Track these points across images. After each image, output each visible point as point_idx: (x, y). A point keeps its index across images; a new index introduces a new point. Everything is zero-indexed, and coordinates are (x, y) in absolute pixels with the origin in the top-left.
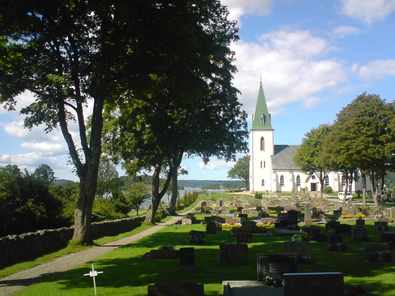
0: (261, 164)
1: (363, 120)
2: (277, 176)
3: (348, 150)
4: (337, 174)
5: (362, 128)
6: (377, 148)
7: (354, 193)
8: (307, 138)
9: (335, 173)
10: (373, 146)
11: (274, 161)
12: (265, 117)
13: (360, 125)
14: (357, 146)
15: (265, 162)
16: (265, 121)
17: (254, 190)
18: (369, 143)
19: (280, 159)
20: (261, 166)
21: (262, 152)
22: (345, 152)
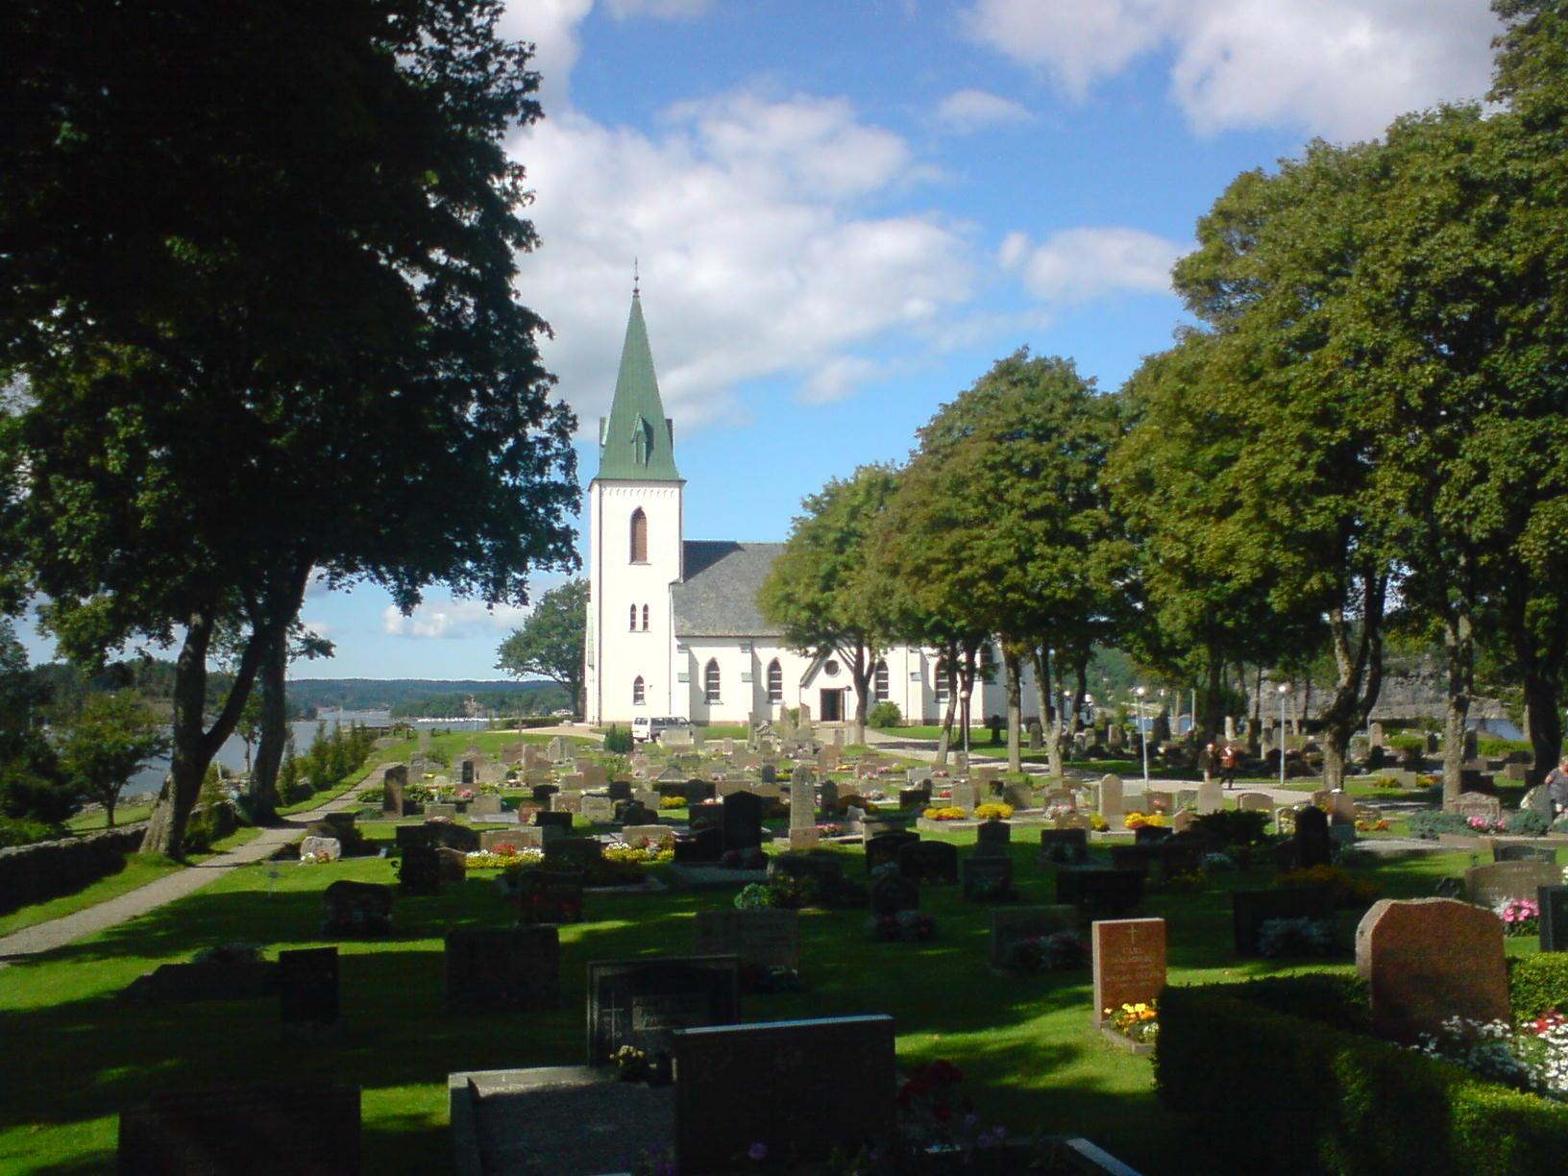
0: (633, 617)
1: (1013, 451)
2: (693, 662)
3: (959, 564)
4: (918, 655)
5: (1007, 482)
6: (1061, 561)
7: (980, 726)
8: (810, 515)
9: (912, 652)
10: (1048, 551)
11: (683, 602)
12: (648, 429)
13: (1001, 471)
14: (989, 551)
15: (646, 608)
16: (650, 446)
17: (604, 719)
18: (1031, 540)
20: (633, 625)
21: (637, 568)
22: (946, 572)
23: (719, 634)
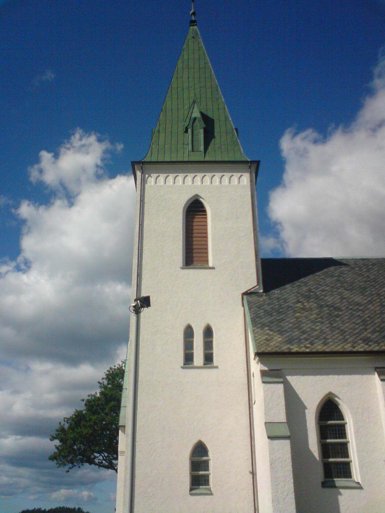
16: (209, 135)
19: (299, 305)
20: (188, 359)
21: (192, 273)
23: (339, 348)
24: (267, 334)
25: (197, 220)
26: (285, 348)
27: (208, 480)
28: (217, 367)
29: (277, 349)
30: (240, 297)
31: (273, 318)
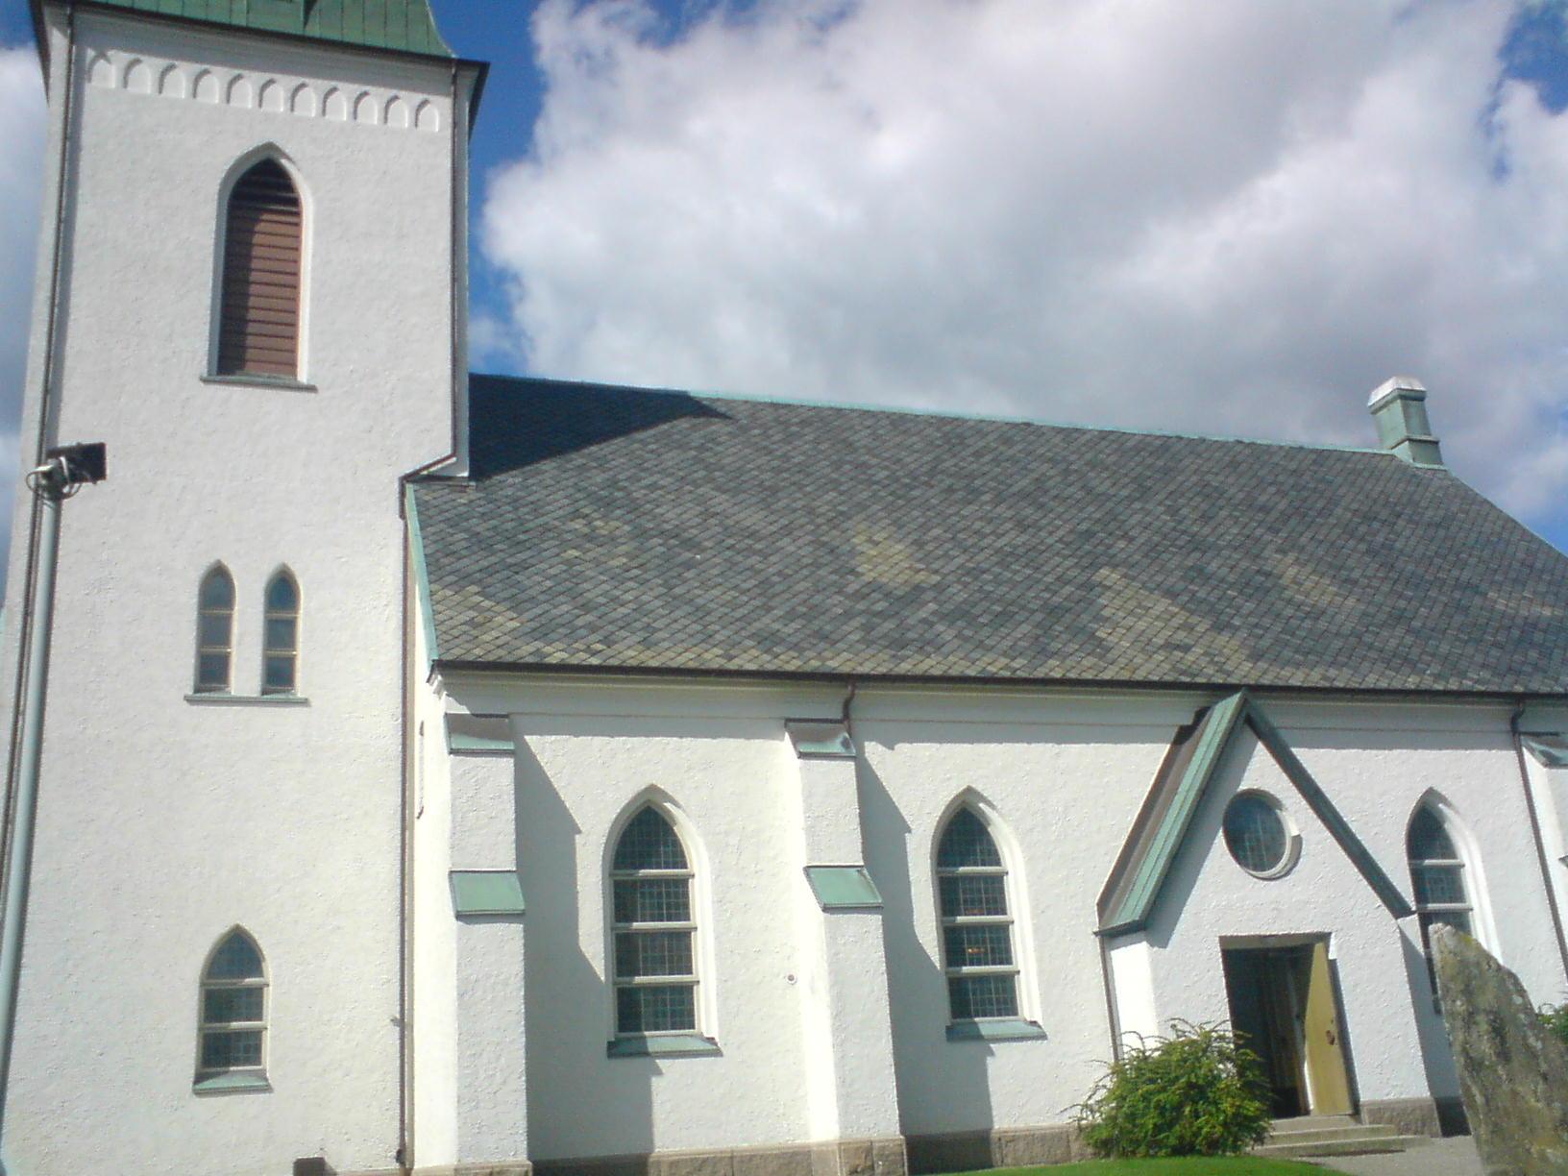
19: (578, 525)
20: (211, 673)
21: (236, 397)
24: (475, 607)
25: (266, 229)
26: (526, 651)
27: (258, 1049)
28: (305, 703)
29: (501, 652)
30: (396, 486)
31: (493, 559)
